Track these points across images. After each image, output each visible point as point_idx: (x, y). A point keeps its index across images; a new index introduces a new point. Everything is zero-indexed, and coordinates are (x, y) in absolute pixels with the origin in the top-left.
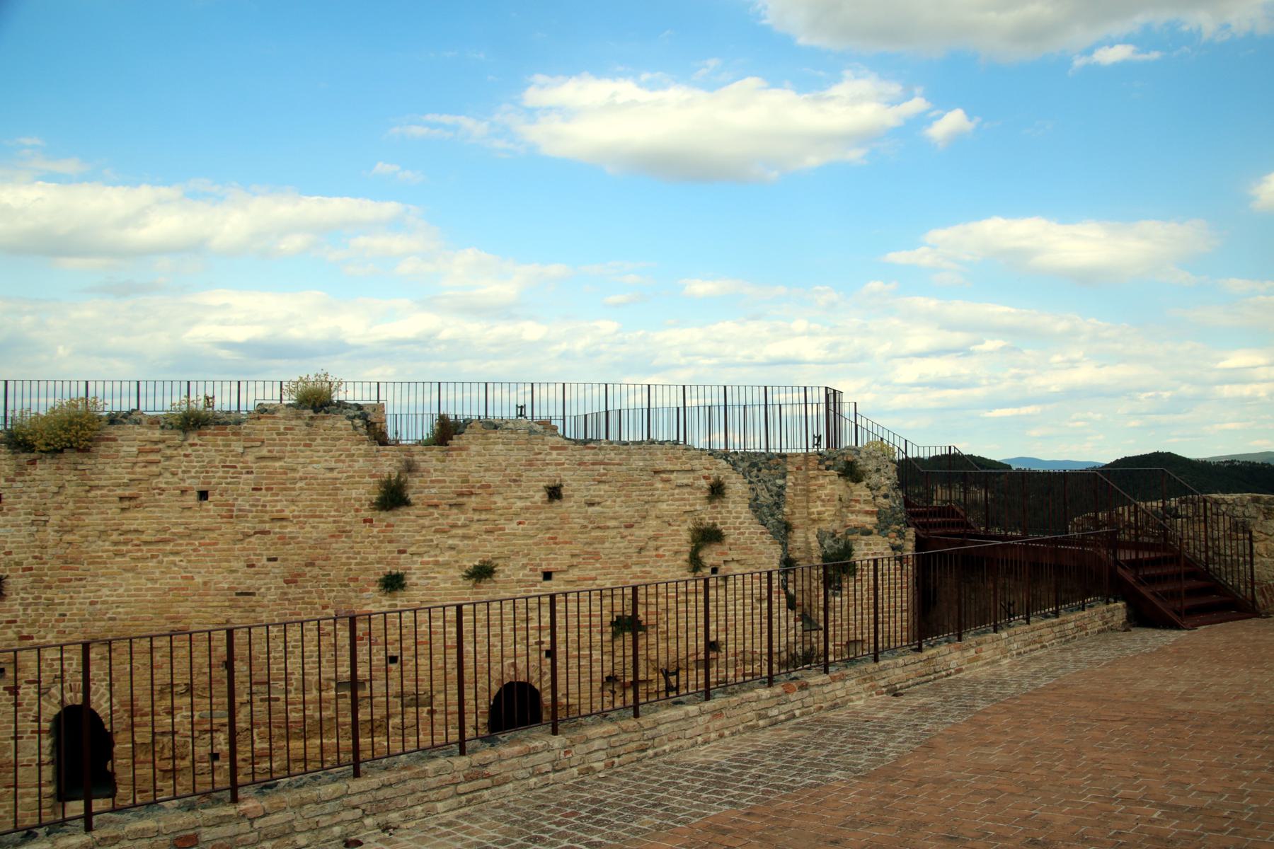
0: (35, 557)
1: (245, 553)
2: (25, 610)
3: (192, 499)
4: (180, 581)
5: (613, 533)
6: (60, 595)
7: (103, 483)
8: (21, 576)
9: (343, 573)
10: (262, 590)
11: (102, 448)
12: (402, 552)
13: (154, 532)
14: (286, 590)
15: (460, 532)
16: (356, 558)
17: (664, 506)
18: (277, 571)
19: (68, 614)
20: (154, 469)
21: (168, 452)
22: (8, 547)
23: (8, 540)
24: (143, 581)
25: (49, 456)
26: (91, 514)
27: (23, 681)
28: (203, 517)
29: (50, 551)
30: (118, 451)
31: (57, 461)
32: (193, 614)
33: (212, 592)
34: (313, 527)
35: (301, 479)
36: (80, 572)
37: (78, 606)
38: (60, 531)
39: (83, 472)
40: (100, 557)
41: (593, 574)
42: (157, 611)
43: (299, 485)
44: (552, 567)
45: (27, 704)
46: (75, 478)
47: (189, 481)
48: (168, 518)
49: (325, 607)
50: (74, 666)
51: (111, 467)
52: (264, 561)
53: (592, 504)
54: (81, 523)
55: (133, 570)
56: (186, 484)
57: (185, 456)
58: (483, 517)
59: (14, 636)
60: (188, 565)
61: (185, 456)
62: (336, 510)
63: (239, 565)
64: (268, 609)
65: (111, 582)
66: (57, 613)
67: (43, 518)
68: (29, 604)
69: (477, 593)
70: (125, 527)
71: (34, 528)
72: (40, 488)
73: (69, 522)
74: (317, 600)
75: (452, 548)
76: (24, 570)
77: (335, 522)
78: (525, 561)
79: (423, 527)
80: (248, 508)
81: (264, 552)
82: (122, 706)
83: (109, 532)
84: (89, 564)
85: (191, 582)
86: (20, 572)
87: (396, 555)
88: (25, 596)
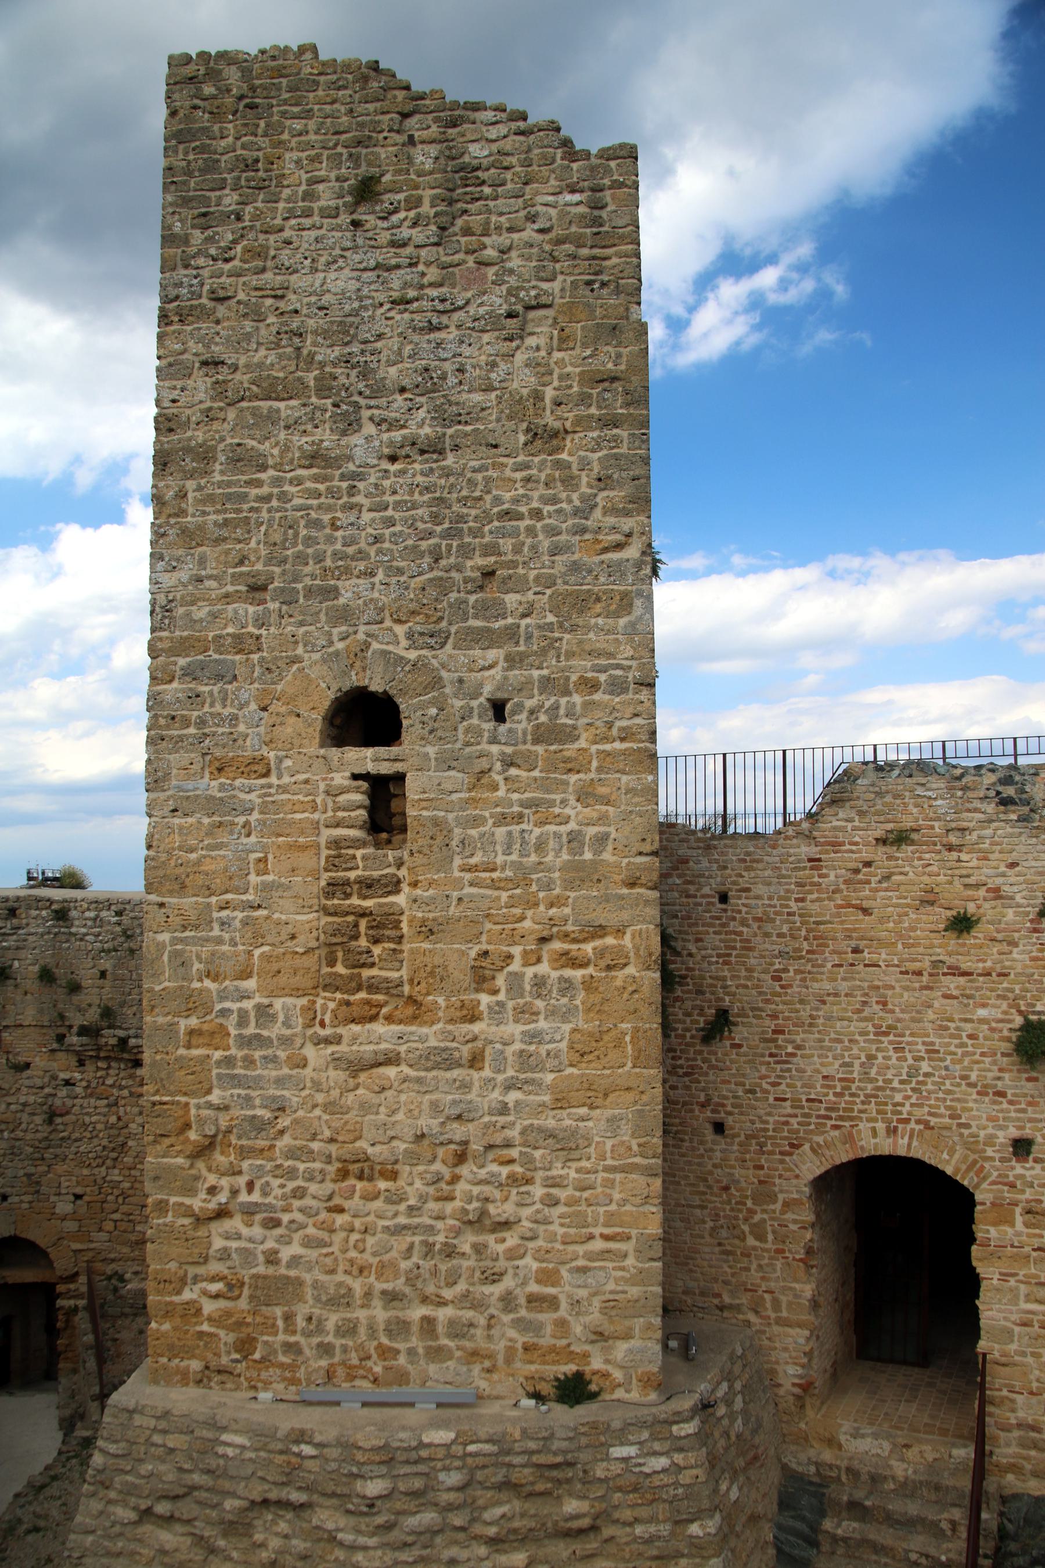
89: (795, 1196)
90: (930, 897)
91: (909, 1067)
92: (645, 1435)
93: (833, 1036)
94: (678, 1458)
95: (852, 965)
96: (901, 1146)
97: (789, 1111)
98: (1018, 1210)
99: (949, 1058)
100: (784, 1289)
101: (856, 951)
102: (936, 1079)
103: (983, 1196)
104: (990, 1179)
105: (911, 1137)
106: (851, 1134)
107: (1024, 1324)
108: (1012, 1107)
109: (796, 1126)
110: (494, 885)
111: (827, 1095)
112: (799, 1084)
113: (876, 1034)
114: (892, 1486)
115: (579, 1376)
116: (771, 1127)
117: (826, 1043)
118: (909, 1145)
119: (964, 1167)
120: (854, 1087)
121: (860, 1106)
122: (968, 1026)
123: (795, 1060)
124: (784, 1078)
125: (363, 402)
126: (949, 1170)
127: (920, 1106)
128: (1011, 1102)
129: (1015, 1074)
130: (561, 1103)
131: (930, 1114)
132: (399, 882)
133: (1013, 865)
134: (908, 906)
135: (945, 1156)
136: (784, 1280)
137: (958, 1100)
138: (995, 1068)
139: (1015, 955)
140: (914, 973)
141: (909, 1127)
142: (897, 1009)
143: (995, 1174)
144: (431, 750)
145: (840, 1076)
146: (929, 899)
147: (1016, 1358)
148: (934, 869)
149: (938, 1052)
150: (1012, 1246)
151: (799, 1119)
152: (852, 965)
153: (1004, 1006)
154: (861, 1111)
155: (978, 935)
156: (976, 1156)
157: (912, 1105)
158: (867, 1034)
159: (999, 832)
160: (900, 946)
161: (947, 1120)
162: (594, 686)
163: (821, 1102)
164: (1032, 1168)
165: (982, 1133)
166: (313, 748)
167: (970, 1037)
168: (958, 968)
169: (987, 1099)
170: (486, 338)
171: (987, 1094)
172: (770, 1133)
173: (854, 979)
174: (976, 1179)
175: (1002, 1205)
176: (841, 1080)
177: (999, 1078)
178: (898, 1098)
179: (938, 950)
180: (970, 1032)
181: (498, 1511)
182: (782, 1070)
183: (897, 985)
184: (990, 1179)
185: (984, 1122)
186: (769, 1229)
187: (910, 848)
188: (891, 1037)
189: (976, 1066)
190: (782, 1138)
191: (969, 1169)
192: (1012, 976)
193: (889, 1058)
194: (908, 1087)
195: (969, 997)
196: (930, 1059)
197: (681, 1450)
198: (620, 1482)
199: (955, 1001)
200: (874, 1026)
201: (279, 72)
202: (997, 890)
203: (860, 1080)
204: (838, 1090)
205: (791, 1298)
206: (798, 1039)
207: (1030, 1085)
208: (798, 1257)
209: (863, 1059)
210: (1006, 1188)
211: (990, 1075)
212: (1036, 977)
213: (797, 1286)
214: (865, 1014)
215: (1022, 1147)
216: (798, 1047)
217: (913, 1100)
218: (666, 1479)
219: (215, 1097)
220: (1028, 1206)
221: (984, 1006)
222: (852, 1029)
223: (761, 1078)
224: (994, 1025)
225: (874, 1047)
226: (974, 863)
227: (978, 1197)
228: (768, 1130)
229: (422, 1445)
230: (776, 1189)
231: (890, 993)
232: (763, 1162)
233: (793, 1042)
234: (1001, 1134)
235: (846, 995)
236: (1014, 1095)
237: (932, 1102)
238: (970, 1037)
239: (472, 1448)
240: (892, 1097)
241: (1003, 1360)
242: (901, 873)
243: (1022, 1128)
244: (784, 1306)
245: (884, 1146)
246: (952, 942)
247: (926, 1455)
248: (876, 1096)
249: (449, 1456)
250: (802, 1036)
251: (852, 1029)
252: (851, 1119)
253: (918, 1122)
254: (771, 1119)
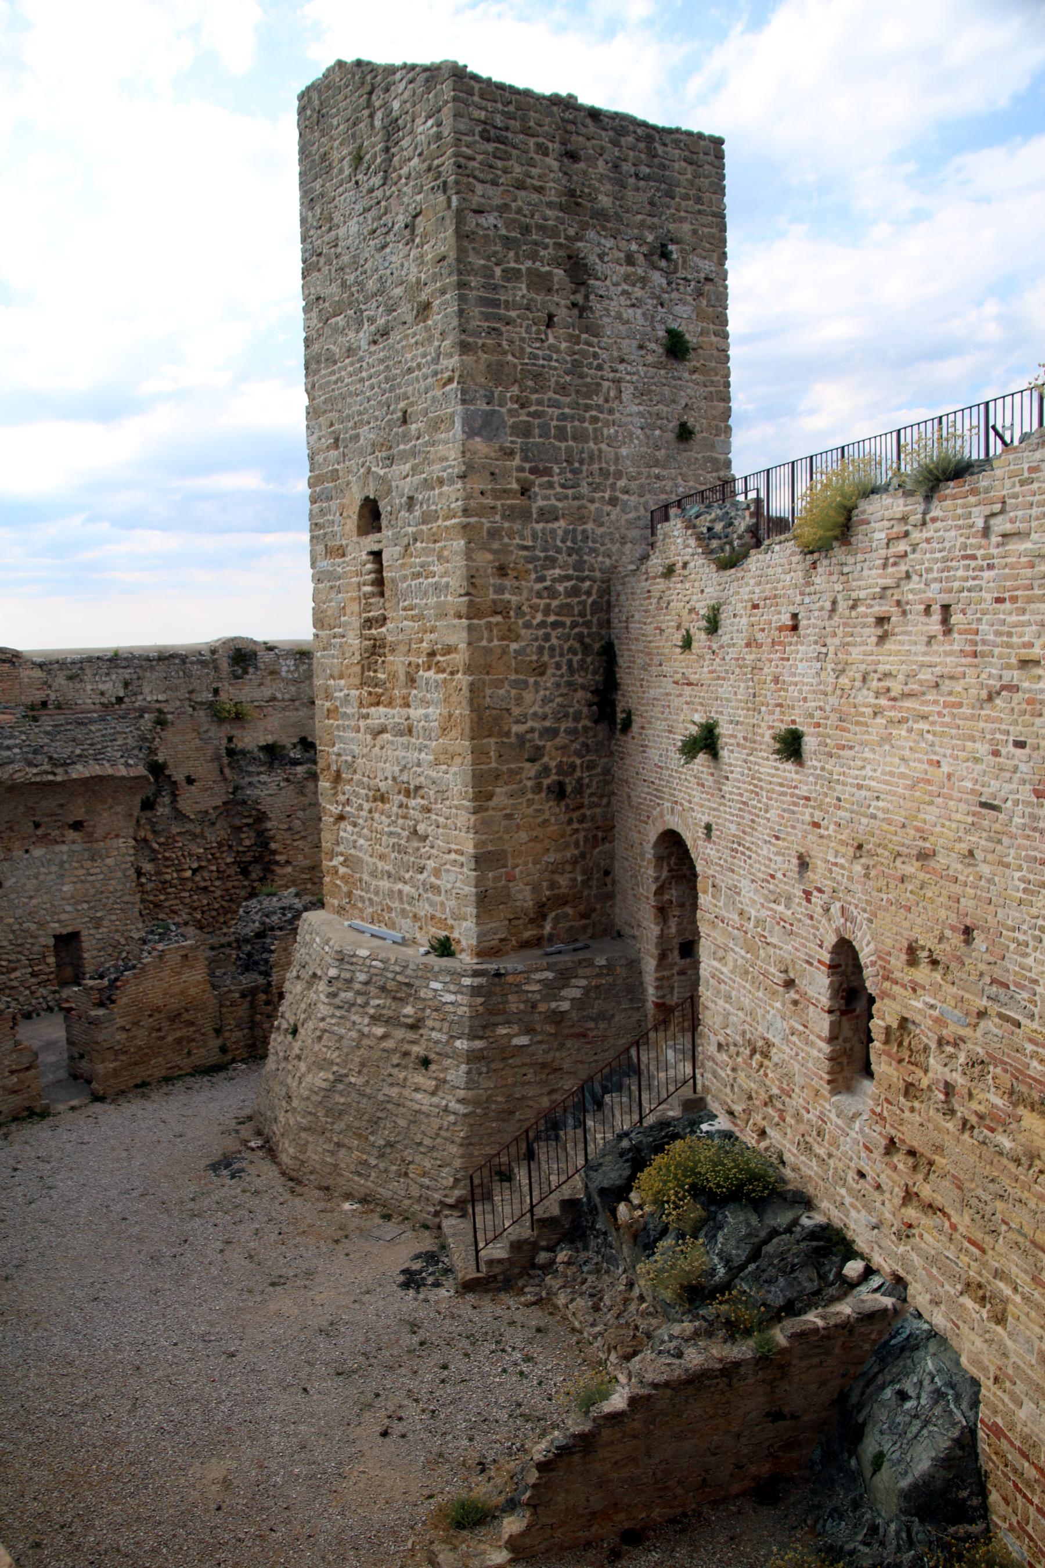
32: (938, 829)
33: (956, 794)
92: (448, 979)
94: (459, 997)
110: (412, 618)
115: (448, 939)
125: (363, 307)
130: (437, 763)
132: (385, 619)
144: (390, 533)
162: (441, 482)
166: (355, 539)
170: (400, 245)
181: (377, 1002)
197: (462, 993)
198: (430, 1003)
201: (328, 87)
218: (452, 1009)
219: (335, 749)
229: (355, 955)
239: (374, 963)
249: (363, 964)
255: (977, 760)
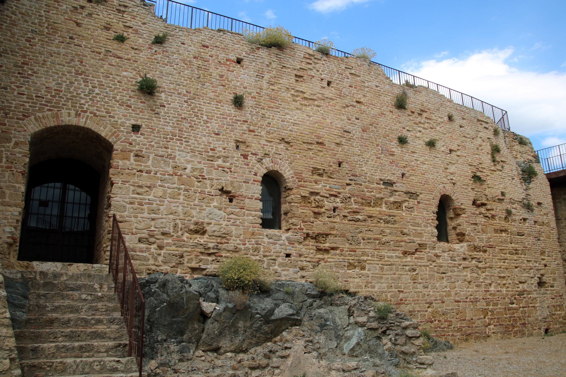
0: (257, 93)
1: (347, 113)
2: (252, 117)
3: (325, 84)
4: (321, 119)
5: (469, 140)
6: (268, 113)
7: (287, 66)
8: (251, 100)
9: (384, 132)
10: (354, 132)
11: (288, 51)
12: (404, 128)
13: (310, 94)
14: (363, 134)
15: (422, 126)
16: (388, 127)
17: (481, 134)
18: (359, 124)
19: (272, 123)
20: (309, 66)
21: (316, 61)
22: (245, 85)
23: (246, 81)
24: (305, 116)
25: (266, 48)
26: (283, 79)
27: (250, 153)
28: (330, 93)
29: (264, 91)
30: (295, 54)
31: (269, 51)
32: (326, 136)
34: (372, 109)
35: (367, 87)
36: (277, 105)
37: (276, 120)
38: (269, 83)
39: (280, 59)
40: (287, 100)
41: (465, 155)
42: (311, 131)
43: (366, 89)
44: (453, 148)
45: (252, 165)
46: (277, 61)
47: (324, 75)
48: (316, 89)
49: (378, 145)
50: (274, 150)
51: (292, 60)
52: (354, 119)
53: (461, 127)
54: (278, 82)
55: (300, 109)
56: (323, 76)
57: (323, 64)
58: (429, 121)
59: (246, 129)
60: (324, 113)
61: (323, 64)
62: (380, 104)
63: (344, 118)
64: (356, 141)
65: (291, 113)
66: (266, 122)
67: (262, 75)
68: (254, 115)
69: (430, 153)
70: (297, 89)
71: (258, 79)
72: (261, 61)
73: (273, 80)
74: (374, 142)
75: (420, 132)
76: (252, 98)
77: (380, 109)
78: (444, 143)
79: (410, 120)
80: (347, 93)
81: (354, 115)
82: (295, 175)
83: (290, 90)
84: (281, 102)
85: (325, 120)
86: (250, 98)
87: (402, 129)
88: (252, 110)
89: (22, 140)
90: (109, 26)
91: (90, 90)
93: (54, 70)
95: (68, 43)
96: (81, 122)
97: (25, 100)
98: (132, 154)
99: (108, 89)
100: (8, 187)
101: (71, 38)
102: (101, 96)
103: (117, 146)
104: (121, 140)
105: (87, 119)
106: (57, 114)
107: (131, 203)
108: (133, 112)
109: (28, 107)
111: (47, 95)
112: (32, 89)
113: (75, 74)
114: (65, 278)
116: (13, 106)
117: (50, 73)
118: (86, 122)
119: (110, 134)
120: (61, 94)
121: (63, 103)
122: (118, 78)
123: (32, 78)
124: (25, 85)
126: (103, 134)
127: (93, 106)
128: (133, 110)
129: (136, 99)
131: (97, 110)
133: (144, 24)
134: (98, 27)
135: (102, 128)
136: (10, 182)
137: (111, 106)
138: (128, 96)
139: (140, 55)
140: (97, 52)
141: (86, 114)
142: (87, 65)
143: (124, 138)
145: (55, 88)
146: (107, 28)
147: (127, 218)
148: (112, 16)
149: (104, 85)
150: (128, 169)
151: (30, 104)
152: (68, 43)
153: (134, 73)
154: (63, 105)
155: (126, 45)
156: (116, 130)
157: (89, 105)
158: (71, 73)
159: (140, 11)
160: (92, 41)
161: (104, 114)
163: (43, 98)
164: (140, 137)
165: (120, 121)
167: (119, 82)
168: (117, 55)
169: (123, 107)
171: (123, 106)
172: (13, 109)
173: (69, 49)
174: (115, 139)
175: (125, 152)
176: (55, 90)
177: (129, 100)
178: (83, 101)
179: (109, 47)
180: (119, 80)
182: (24, 81)
183: (89, 56)
184: (121, 140)
185: (121, 116)
186: (4, 155)
187: (102, 7)
188: (83, 76)
189: (120, 94)
190: (21, 112)
191: (113, 135)
192: (139, 62)
193: (81, 84)
194: (88, 98)
195: (120, 67)
196: (99, 88)
199: (114, 67)
200: (75, 70)
202: (137, 31)
203: (65, 91)
204: (53, 94)
205: (12, 191)
206: (35, 69)
207: (142, 104)
208: (19, 171)
209: (68, 83)
210: (128, 144)
211: (125, 98)
212: (148, 64)
213: (17, 185)
214: (71, 64)
215: (136, 128)
216: (35, 73)
217: (90, 103)
220: (137, 153)
221: (126, 71)
222: (64, 69)
223: (11, 83)
224: (129, 79)
225: (74, 79)
226: (129, 19)
227: (115, 147)
228: (12, 107)
230: (12, 136)
231: (85, 58)
232: (6, 121)
233: (32, 69)
234: (128, 122)
235: (64, 55)
236: (134, 107)
237: (99, 105)
238: (119, 82)
240: (80, 101)
241: (121, 219)
242: (98, 15)
243: (137, 121)
244: (7, 195)
245: (74, 121)
246: (116, 45)
247: (80, 268)
248: (72, 100)
250: (38, 68)
251: (64, 69)
252: (59, 107)
253: (91, 113)
254: (14, 102)
255: (343, 120)
